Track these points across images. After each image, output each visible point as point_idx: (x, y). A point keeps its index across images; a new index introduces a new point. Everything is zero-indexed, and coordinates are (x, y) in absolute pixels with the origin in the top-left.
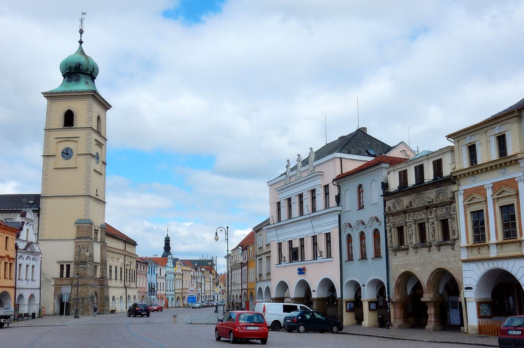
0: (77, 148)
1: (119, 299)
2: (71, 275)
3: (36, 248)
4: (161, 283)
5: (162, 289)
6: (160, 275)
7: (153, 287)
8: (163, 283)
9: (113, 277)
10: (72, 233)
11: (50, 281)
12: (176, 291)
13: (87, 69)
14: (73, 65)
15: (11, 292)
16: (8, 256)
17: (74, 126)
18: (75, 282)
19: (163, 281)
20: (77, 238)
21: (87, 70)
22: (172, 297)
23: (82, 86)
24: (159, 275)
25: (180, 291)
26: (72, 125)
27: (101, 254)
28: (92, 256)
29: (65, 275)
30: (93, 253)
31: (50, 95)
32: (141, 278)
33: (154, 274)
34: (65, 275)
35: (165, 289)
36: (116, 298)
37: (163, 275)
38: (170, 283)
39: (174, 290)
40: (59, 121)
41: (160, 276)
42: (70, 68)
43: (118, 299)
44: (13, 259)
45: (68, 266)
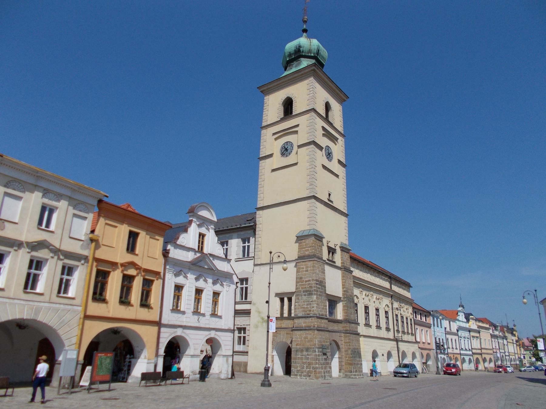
4: (452, 340)
5: (454, 347)
6: (451, 330)
7: (442, 344)
8: (455, 340)
12: (474, 351)
13: (309, 50)
19: (454, 337)
20: (300, 258)
21: (310, 51)
22: (469, 357)
24: (448, 329)
25: (479, 351)
26: (291, 113)
27: (343, 285)
30: (325, 279)
31: (268, 90)
32: (423, 331)
33: (441, 327)
35: (458, 347)
37: (454, 330)
38: (464, 340)
39: (470, 348)
41: (450, 331)
43: (383, 355)
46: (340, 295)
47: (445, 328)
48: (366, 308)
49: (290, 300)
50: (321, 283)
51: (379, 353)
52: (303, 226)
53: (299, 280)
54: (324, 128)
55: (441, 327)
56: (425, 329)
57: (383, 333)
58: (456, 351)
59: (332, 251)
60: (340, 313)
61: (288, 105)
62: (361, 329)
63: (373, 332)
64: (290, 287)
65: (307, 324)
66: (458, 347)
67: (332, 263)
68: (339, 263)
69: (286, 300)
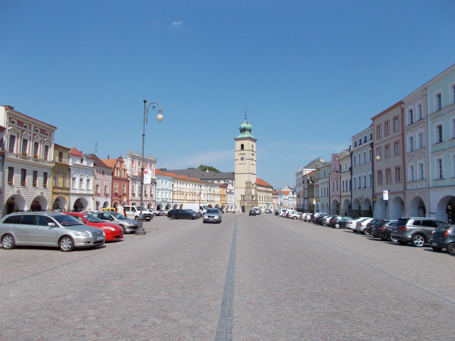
0: (245, 157)
3: (233, 191)
9: (261, 200)
10: (245, 186)
14: (243, 128)
15: (225, 205)
16: (224, 195)
17: (244, 150)
21: (248, 129)
23: (247, 135)
26: (243, 149)
40: (239, 148)
42: (242, 129)
44: (225, 195)
46: (254, 195)
48: (260, 196)
49: (244, 196)
50: (251, 193)
51: (262, 207)
52: (247, 180)
54: (252, 154)
56: (276, 199)
57: (264, 202)
59: (253, 185)
60: (254, 199)
61: (242, 146)
62: (259, 202)
63: (261, 202)
64: (244, 194)
67: (253, 188)
68: (254, 187)
69: (243, 196)
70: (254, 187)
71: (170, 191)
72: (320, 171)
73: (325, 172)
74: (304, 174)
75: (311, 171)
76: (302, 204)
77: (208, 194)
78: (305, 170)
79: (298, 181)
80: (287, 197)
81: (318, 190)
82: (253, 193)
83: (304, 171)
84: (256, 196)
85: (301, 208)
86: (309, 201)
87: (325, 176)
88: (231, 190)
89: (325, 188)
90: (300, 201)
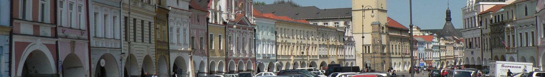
1: (399, 64)
2: (371, 52)
11: (360, 55)
18: (373, 55)
20: (372, 32)
25: (445, 58)
28: (381, 41)
29: (367, 52)
30: (381, 40)
33: (423, 47)
34: (367, 52)
36: (397, 64)
45: (369, 47)
47: (425, 48)
53: (374, 40)
55: (423, 47)
58: (430, 59)
60: (385, 51)
65: (377, 56)
66: (431, 57)
68: (385, 32)
70: (385, 32)
71: (273, 42)
72: (517, 7)
73: (526, 8)
74: (481, 11)
75: (494, 5)
76: (479, 58)
77: (320, 45)
78: (483, 5)
79: (467, 21)
80: (430, 46)
81: (513, 36)
82: (384, 42)
83: (481, 6)
84: (389, 45)
85: (476, 64)
86: (493, 52)
87: (526, 14)
88: (350, 38)
89: (527, 33)
90: (472, 53)
